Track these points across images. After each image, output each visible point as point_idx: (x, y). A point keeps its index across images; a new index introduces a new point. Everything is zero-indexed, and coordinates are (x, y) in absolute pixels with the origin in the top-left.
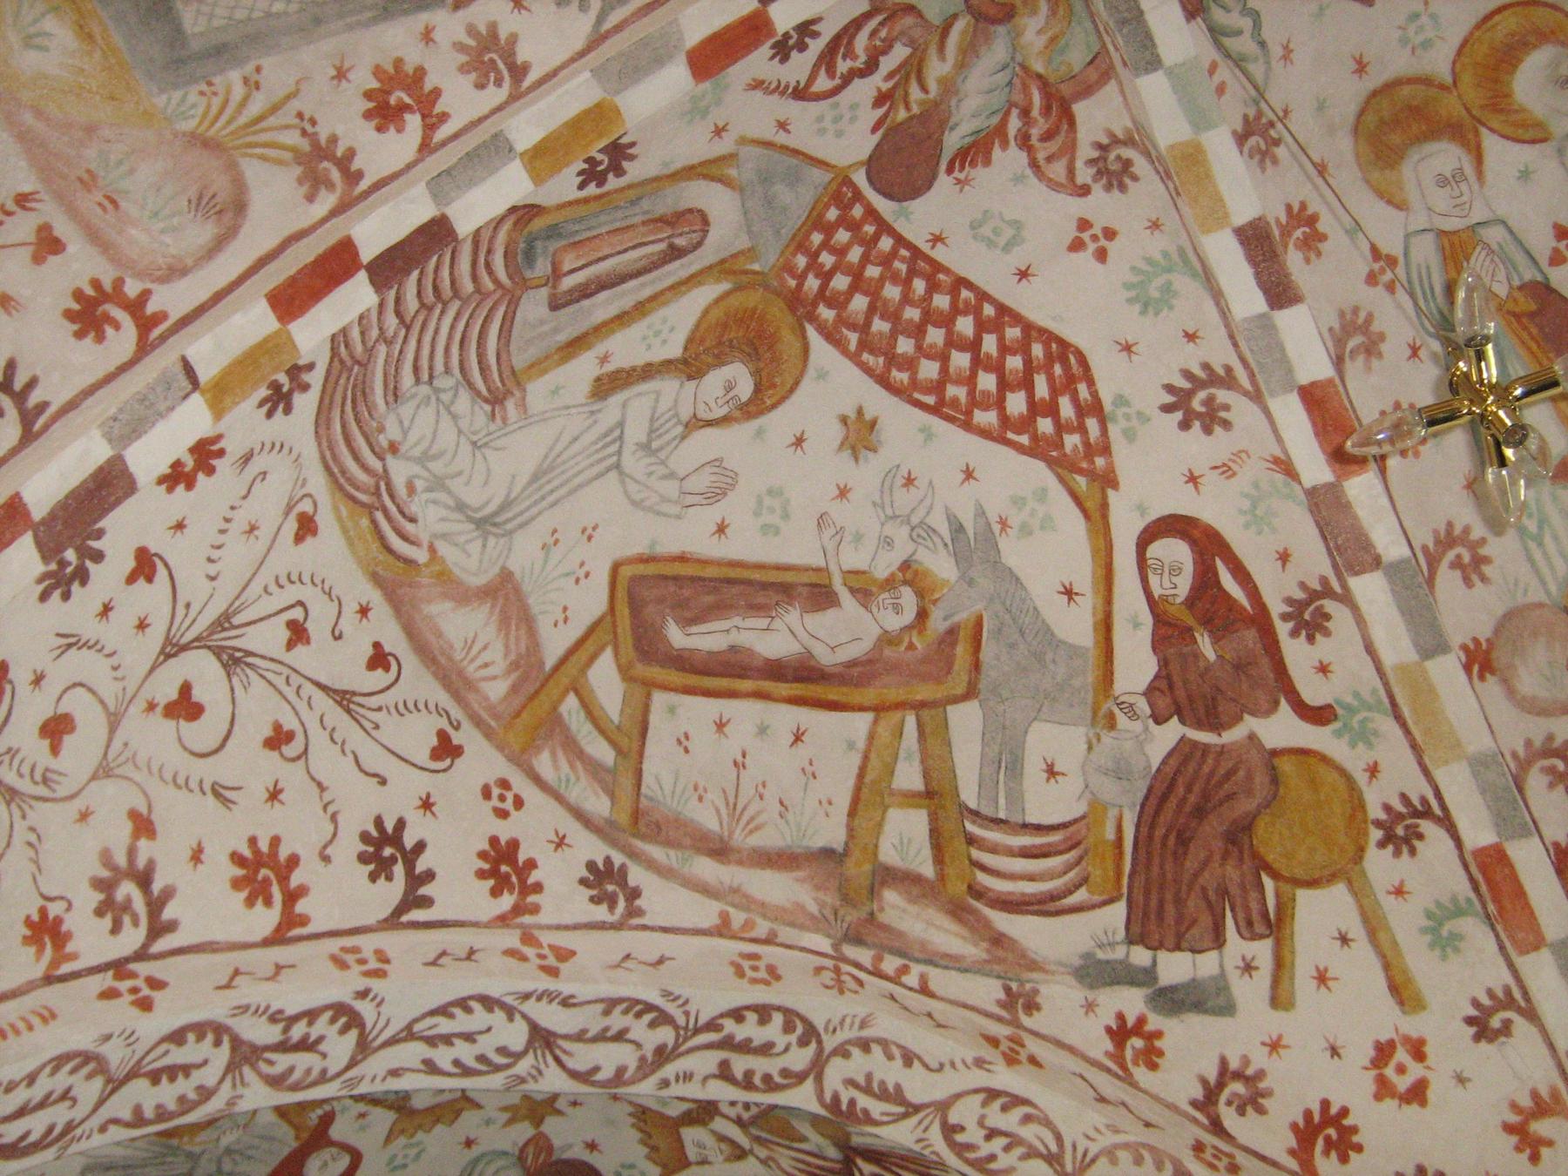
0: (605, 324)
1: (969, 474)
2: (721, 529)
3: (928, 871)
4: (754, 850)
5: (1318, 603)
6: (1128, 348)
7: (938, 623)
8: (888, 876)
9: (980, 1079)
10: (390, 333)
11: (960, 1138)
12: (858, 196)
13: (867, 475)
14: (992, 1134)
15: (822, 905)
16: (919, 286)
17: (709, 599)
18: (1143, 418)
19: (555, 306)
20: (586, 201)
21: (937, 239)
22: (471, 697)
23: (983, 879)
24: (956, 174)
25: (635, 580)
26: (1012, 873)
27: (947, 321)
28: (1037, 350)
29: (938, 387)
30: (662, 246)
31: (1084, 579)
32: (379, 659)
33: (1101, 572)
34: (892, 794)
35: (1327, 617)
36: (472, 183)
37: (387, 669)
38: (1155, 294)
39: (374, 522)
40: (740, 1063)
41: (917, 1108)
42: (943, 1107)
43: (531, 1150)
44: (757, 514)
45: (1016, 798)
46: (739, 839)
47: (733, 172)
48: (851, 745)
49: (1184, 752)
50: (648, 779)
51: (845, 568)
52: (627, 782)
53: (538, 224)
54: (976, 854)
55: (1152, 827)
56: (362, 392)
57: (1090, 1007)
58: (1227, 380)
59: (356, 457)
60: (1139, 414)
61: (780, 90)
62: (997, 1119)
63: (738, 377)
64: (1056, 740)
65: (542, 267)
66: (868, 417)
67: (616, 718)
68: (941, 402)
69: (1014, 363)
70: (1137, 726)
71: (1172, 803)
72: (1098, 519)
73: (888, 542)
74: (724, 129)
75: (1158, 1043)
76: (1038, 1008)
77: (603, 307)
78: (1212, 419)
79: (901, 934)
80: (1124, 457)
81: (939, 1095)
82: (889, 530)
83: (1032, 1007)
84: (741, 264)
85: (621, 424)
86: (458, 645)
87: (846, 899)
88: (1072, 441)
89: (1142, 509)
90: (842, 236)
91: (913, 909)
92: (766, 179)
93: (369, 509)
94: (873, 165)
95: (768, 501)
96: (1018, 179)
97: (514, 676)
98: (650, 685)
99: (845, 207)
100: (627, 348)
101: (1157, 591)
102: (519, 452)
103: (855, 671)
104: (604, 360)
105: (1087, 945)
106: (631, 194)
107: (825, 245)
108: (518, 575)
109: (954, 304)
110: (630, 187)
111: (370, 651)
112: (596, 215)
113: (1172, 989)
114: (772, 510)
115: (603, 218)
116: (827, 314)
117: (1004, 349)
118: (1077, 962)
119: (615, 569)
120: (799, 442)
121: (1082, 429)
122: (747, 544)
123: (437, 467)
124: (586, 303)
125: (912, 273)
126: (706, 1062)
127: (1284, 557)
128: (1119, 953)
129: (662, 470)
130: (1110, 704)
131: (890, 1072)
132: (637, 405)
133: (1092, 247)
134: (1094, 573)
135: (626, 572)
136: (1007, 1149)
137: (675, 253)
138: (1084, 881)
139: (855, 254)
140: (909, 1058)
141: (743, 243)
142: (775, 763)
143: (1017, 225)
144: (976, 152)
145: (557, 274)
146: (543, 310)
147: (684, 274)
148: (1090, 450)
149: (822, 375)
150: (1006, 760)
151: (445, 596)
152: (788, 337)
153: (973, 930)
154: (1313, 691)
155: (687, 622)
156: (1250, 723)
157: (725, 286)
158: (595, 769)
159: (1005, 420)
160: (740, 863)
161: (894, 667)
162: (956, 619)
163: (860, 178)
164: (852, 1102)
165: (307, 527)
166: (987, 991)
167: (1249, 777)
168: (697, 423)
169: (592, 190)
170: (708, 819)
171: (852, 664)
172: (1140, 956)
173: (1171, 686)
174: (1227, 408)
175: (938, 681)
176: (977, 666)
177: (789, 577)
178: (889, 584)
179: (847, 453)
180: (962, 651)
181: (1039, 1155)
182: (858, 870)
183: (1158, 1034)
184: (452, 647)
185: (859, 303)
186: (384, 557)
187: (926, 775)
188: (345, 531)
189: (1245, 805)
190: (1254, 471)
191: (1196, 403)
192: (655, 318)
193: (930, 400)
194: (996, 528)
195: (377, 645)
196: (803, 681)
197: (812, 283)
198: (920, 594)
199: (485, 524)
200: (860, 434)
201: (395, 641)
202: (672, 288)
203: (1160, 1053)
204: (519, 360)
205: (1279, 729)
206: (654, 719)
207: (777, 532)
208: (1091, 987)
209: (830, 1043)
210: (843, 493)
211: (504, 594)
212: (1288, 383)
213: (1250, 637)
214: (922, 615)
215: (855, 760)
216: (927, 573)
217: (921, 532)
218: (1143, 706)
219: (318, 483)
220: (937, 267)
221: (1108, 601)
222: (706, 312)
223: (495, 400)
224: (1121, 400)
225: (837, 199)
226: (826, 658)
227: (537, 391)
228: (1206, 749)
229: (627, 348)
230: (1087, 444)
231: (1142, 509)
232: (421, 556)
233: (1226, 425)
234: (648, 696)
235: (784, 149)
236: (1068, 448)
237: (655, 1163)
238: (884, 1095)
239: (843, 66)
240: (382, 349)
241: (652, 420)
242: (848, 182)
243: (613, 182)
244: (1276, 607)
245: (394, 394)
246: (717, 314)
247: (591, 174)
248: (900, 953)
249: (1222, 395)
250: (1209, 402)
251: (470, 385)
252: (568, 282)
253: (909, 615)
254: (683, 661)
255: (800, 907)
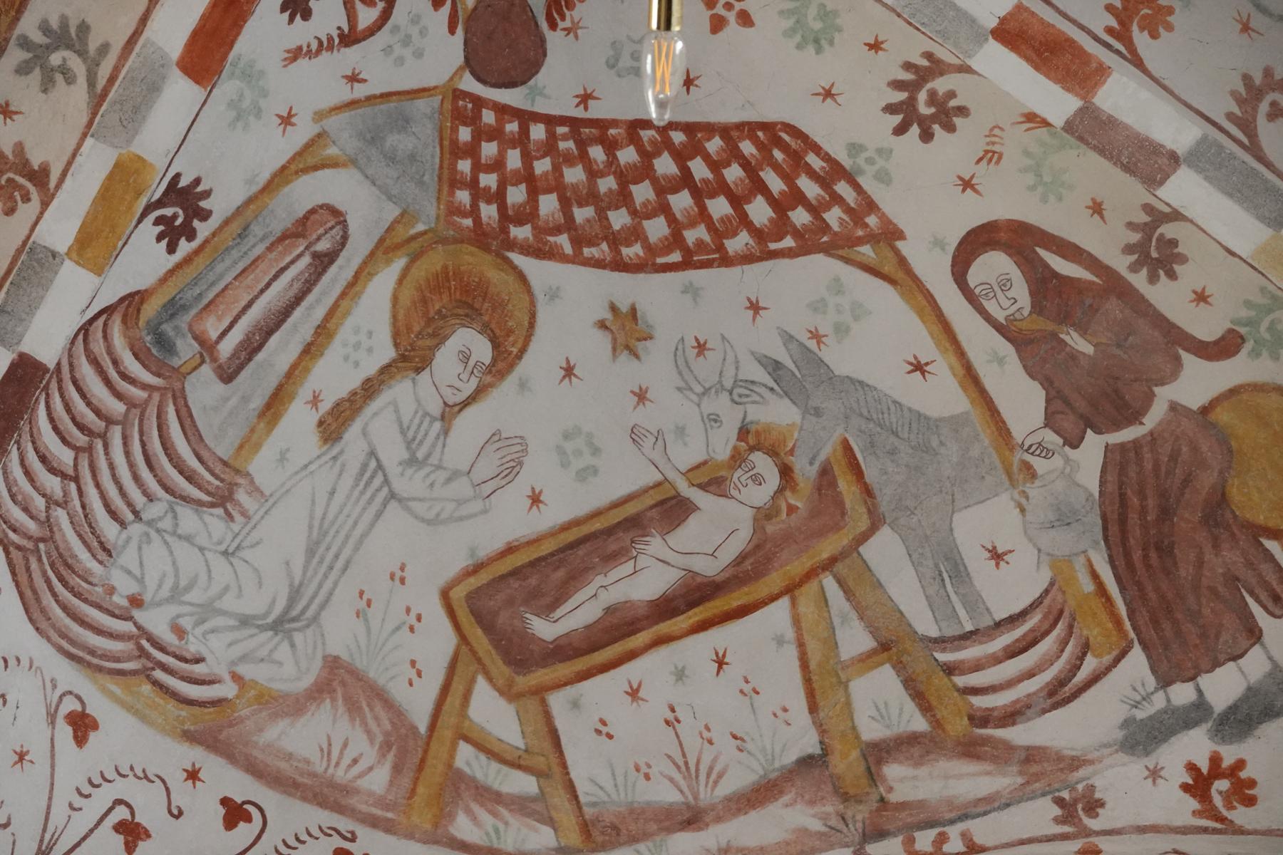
0: (294, 367)
1: (755, 307)
2: (536, 499)
3: (920, 724)
4: (728, 799)
5: (1156, 235)
6: (828, 94)
7: (806, 471)
8: (878, 753)
10: (58, 494)
12: (479, 103)
13: (655, 367)
15: (824, 818)
16: (597, 153)
17: (561, 574)
18: (885, 153)
19: (227, 375)
20: (188, 260)
21: (585, 99)
22: (354, 801)
23: (979, 702)
24: (561, 25)
25: (471, 597)
26: (1005, 679)
27: (644, 171)
28: (747, 148)
29: (676, 240)
30: (306, 260)
31: (925, 345)
32: (234, 813)
33: (937, 329)
34: (845, 666)
35: (1173, 243)
36: (32, 309)
37: (248, 819)
38: (818, 25)
39: (156, 683)
44: (565, 465)
45: (974, 603)
46: (708, 795)
47: (332, 151)
48: (780, 641)
49: (1117, 460)
50: (582, 787)
51: (683, 468)
52: (559, 799)
53: (150, 309)
54: (961, 681)
55: (1127, 555)
56: (64, 565)
57: (1155, 774)
58: (936, 67)
59: (99, 631)
60: (880, 151)
61: (324, 46)
63: (468, 343)
64: (984, 521)
65: (187, 349)
66: (624, 307)
67: (520, 744)
68: (687, 252)
69: (734, 173)
70: (1057, 462)
71: (1133, 518)
72: (902, 277)
73: (715, 419)
74: (290, 115)
75: (1243, 775)
76: (1100, 803)
77: (281, 352)
78: (947, 115)
79: (921, 804)
80: (891, 202)
82: (709, 406)
83: (1094, 806)
84: (402, 233)
85: (372, 454)
86: (315, 757)
87: (846, 798)
88: (834, 217)
89: (939, 243)
90: (489, 150)
91: (923, 771)
92: (373, 138)
93: (145, 673)
94: (474, 62)
95: (569, 446)
97: (390, 757)
98: (540, 692)
99: (473, 120)
100: (334, 377)
101: (1000, 316)
102: (279, 538)
103: (747, 565)
104: (315, 401)
105: (1123, 712)
106: (235, 228)
107: (478, 167)
108: (345, 656)
109: (641, 150)
110: (227, 222)
111: (222, 811)
112: (210, 267)
113: (1233, 709)
114: (578, 453)
115: (220, 268)
116: (521, 233)
117: (716, 166)
118: (1119, 735)
119: (445, 595)
120: (569, 371)
121: (837, 199)
122: (567, 502)
123: (195, 596)
124: (260, 357)
125: (582, 145)
127: (1097, 209)
128: (1159, 701)
129: (441, 476)
130: (1019, 455)
132: (380, 426)
133: (731, 17)
134: (931, 334)
135: (458, 594)
137: (323, 261)
138: (1085, 648)
139: (514, 159)
141: (392, 212)
142: (713, 700)
145: (208, 348)
146: (220, 388)
147: (348, 274)
148: (857, 215)
149: (554, 295)
150: (948, 569)
151: (275, 716)
152: (496, 277)
153: (995, 759)
154: (1206, 326)
155: (547, 610)
156: (1164, 395)
157: (399, 264)
158: (520, 805)
159: (758, 234)
160: (719, 819)
161: (787, 538)
162: (822, 457)
163: (469, 84)
165: (82, 725)
166: (1039, 815)
167: (1195, 449)
168: (450, 412)
169: (184, 247)
170: (665, 793)
171: (742, 558)
172: (1182, 694)
173: (1067, 402)
174: (952, 94)
175: (837, 528)
176: (868, 492)
177: (631, 509)
178: (737, 459)
179: (624, 356)
180: (846, 486)
182: (846, 763)
183: (1240, 764)
184: (308, 762)
185: (548, 204)
186: (185, 712)
187: (874, 632)
188: (130, 708)
189: (1206, 480)
190: (1016, 141)
191: (923, 106)
192: (345, 333)
193: (676, 257)
194: (812, 344)
195: (225, 802)
196: (699, 602)
197: (489, 212)
198: (773, 452)
199: (281, 625)
200: (626, 330)
201: (241, 787)
202: (343, 294)
203: (1252, 783)
204: (223, 448)
205: (1197, 383)
206: (560, 724)
207: (595, 471)
208: (1147, 753)
210: (641, 396)
211: (340, 682)
212: (979, 38)
213: (1113, 307)
214: (786, 472)
215: (792, 652)
216: (768, 429)
217: (740, 390)
218: (1051, 438)
219: (68, 676)
220: (602, 125)
221: (961, 353)
222: (395, 299)
223: (223, 499)
224: (855, 149)
225: (460, 117)
226: (709, 568)
227: (262, 467)
228: (1136, 445)
229: (334, 377)
230: (849, 210)
231: (939, 243)
232: (227, 690)
233: (962, 111)
234: (544, 703)
235: (371, 99)
236: (835, 226)
240: (60, 515)
241: (403, 432)
242: (459, 94)
243: (203, 229)
244: (1120, 263)
245: (105, 550)
246: (408, 295)
247: (172, 234)
248: (930, 824)
249: (941, 85)
250: (933, 98)
251: (186, 499)
252: (226, 348)
253: (773, 480)
254: (562, 651)
255: (804, 831)
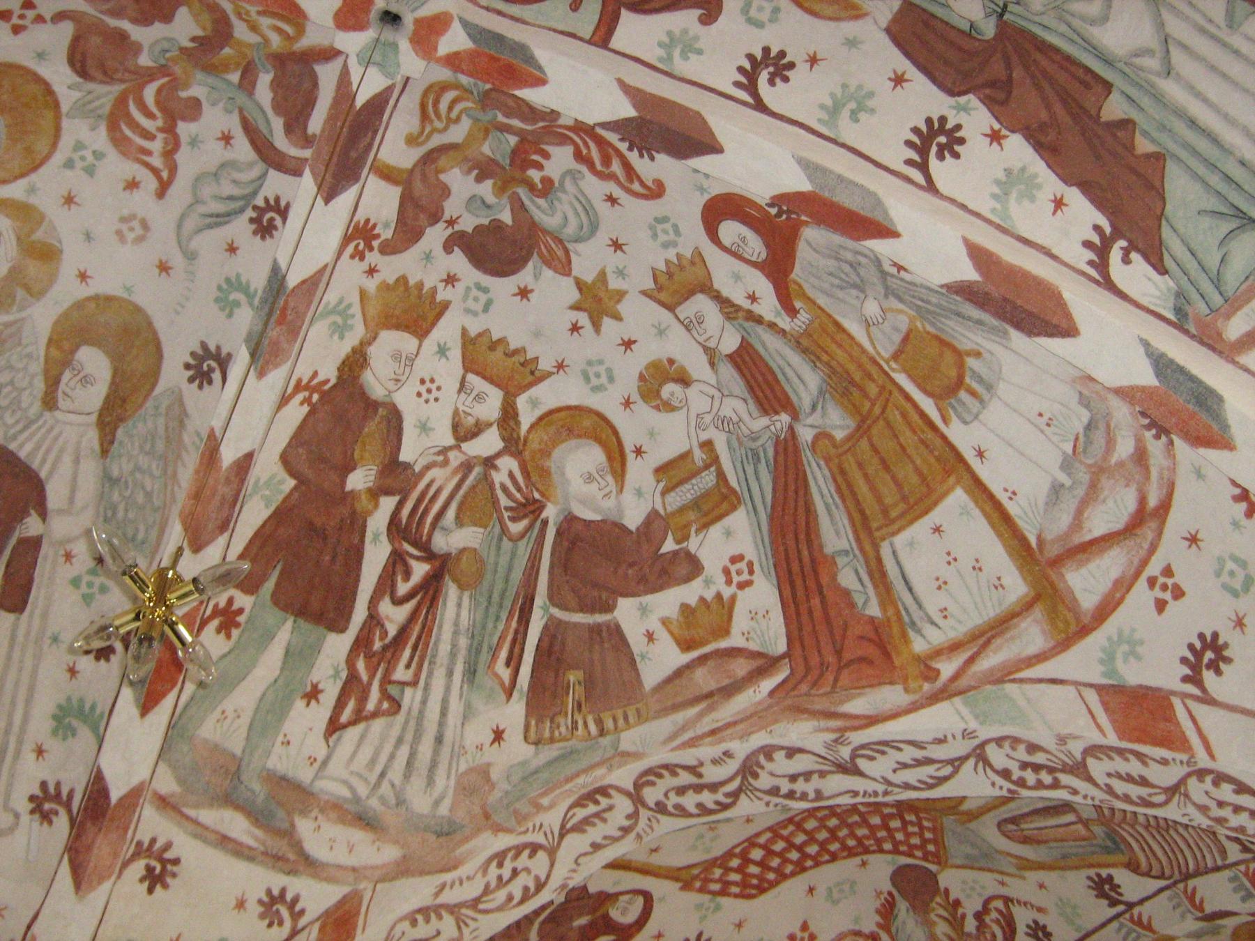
6: (739, 925)
9: (555, 882)
11: (526, 852)
12: (925, 858)
14: (515, 873)
21: (864, 864)
24: (886, 895)
30: (1023, 826)
40: (685, 778)
41: (562, 836)
42: (552, 853)
43: (560, 253)
62: (524, 880)
80: (694, 897)
81: (561, 854)
89: (662, 899)
94: (933, 877)
96: (857, 920)
101: (622, 898)
126: (712, 774)
131: (596, 833)
136: (500, 878)
140: (596, 847)
143: (836, 902)
144: (887, 910)
164: (597, 802)
181: (482, 896)
209: (644, 813)
237: (480, 335)
238: (586, 821)
239: (994, 915)
242: (939, 863)
